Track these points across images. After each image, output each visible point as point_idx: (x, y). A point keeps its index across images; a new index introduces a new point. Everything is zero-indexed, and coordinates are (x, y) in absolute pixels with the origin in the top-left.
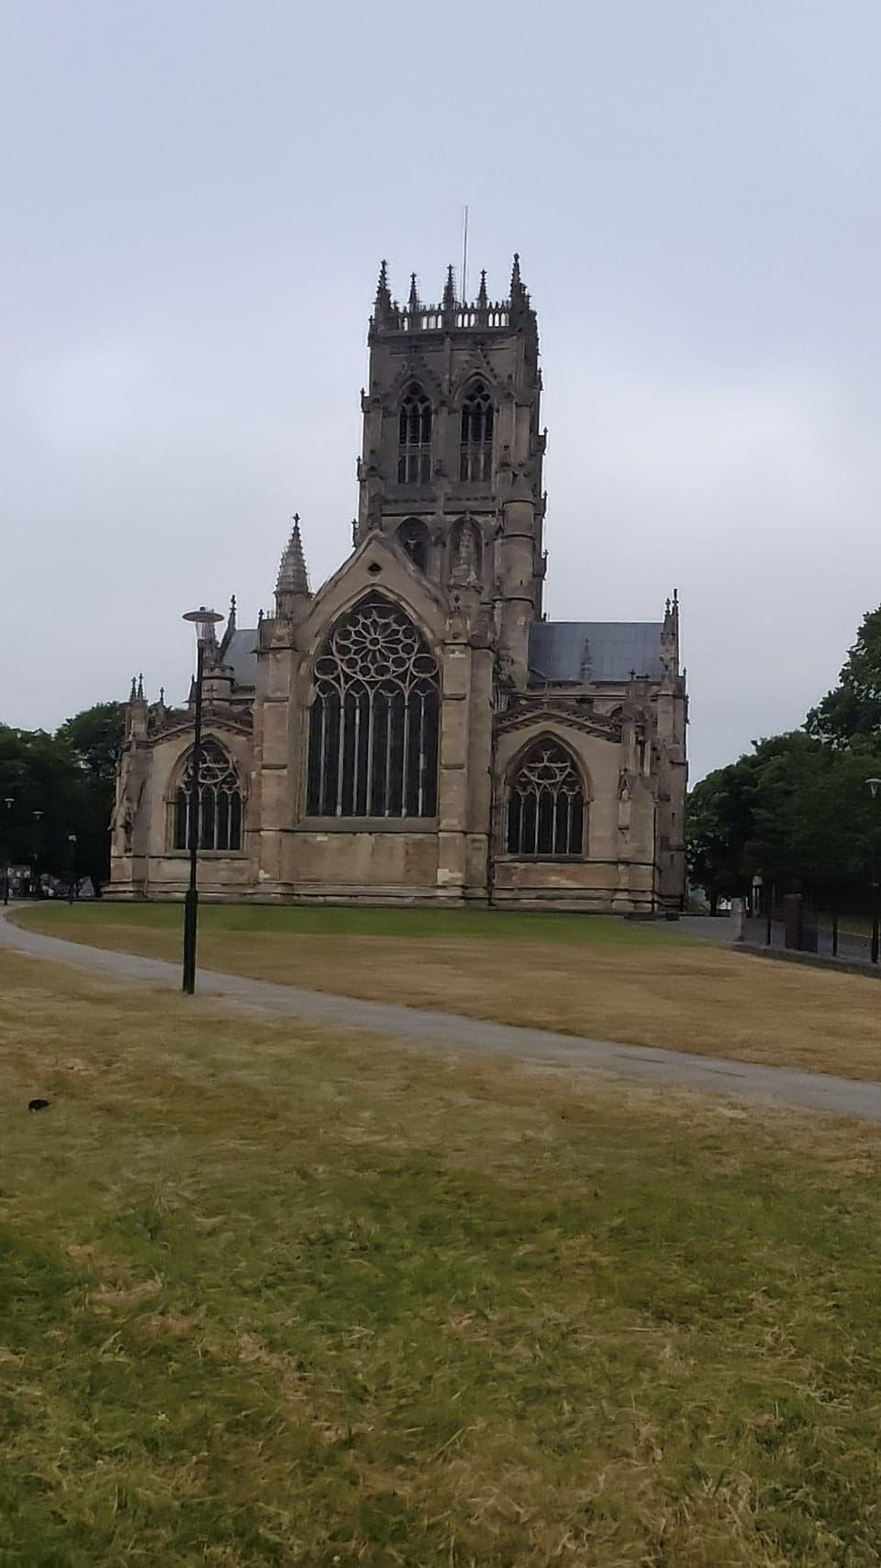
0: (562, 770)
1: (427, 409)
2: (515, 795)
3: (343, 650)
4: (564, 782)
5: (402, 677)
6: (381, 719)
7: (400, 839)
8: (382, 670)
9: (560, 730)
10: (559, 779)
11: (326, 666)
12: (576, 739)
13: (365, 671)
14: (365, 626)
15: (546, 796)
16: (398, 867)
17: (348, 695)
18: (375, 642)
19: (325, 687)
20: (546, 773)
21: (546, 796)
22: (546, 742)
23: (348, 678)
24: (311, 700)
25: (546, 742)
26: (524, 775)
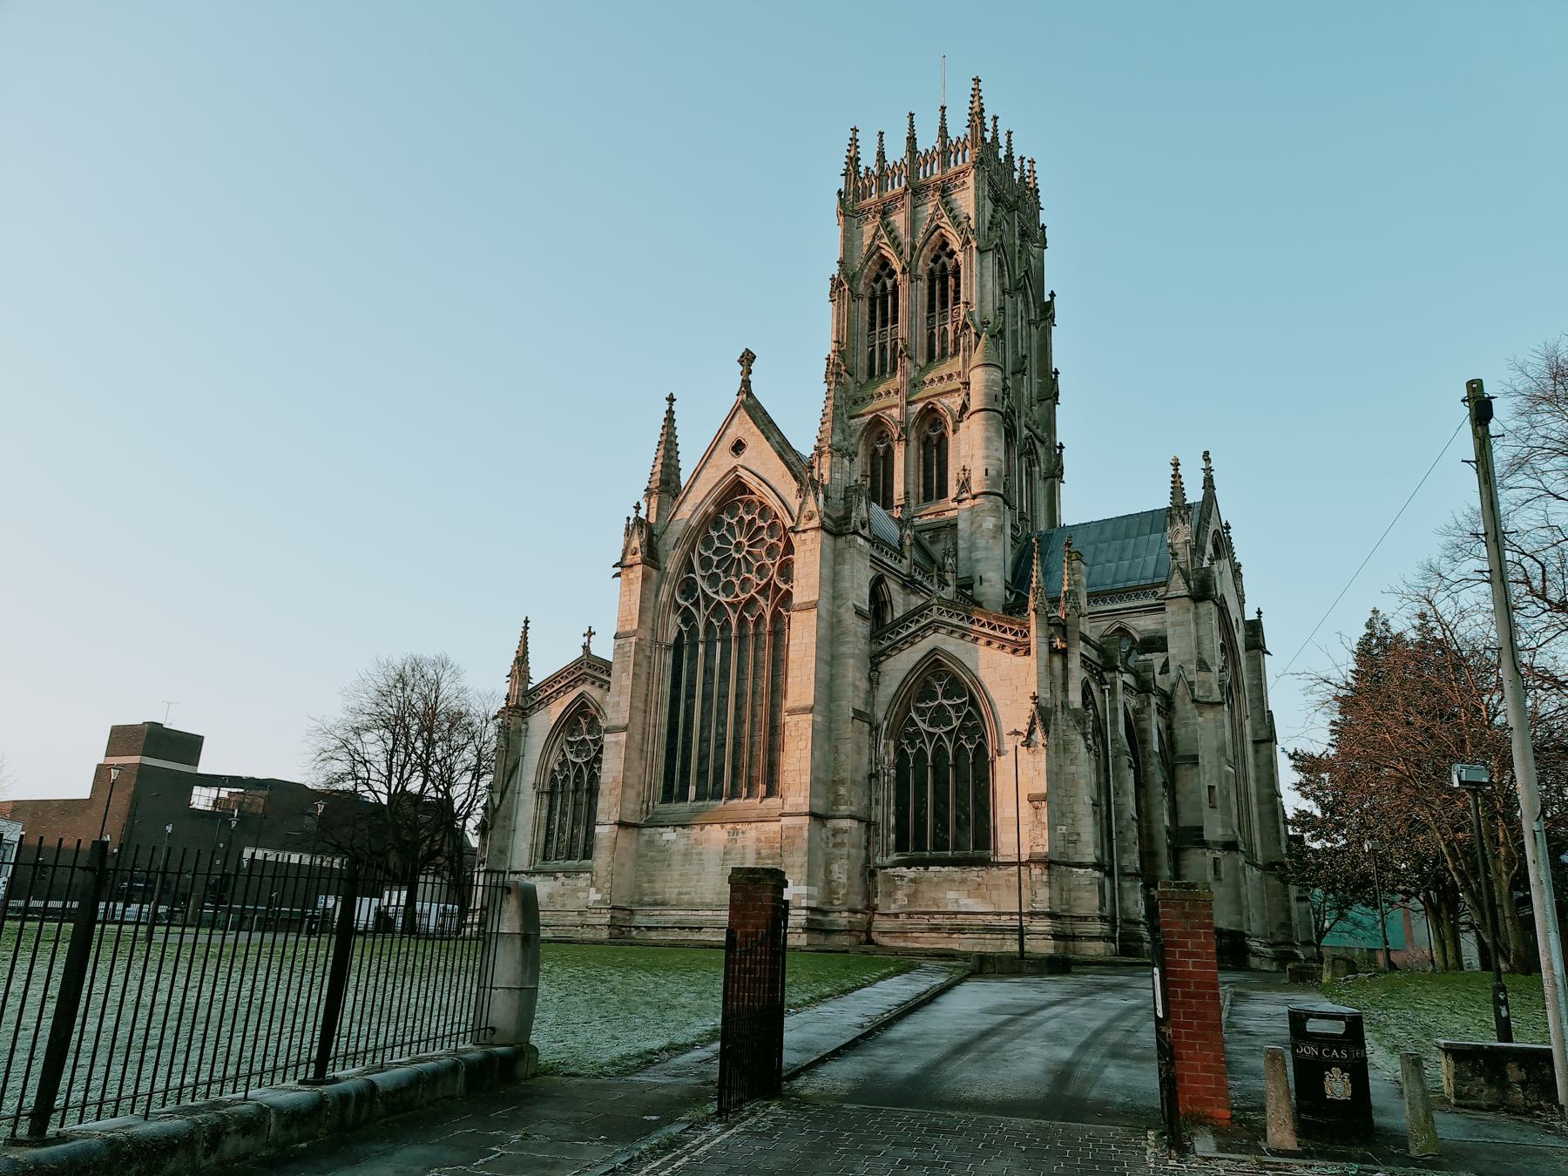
0: (958, 708)
2: (901, 753)
3: (706, 563)
4: (962, 728)
5: (763, 591)
9: (951, 645)
10: (956, 723)
11: (688, 588)
14: (730, 527)
15: (939, 751)
17: (709, 625)
18: (739, 546)
19: (688, 618)
21: (939, 751)
22: (934, 664)
25: (934, 664)
26: (912, 723)
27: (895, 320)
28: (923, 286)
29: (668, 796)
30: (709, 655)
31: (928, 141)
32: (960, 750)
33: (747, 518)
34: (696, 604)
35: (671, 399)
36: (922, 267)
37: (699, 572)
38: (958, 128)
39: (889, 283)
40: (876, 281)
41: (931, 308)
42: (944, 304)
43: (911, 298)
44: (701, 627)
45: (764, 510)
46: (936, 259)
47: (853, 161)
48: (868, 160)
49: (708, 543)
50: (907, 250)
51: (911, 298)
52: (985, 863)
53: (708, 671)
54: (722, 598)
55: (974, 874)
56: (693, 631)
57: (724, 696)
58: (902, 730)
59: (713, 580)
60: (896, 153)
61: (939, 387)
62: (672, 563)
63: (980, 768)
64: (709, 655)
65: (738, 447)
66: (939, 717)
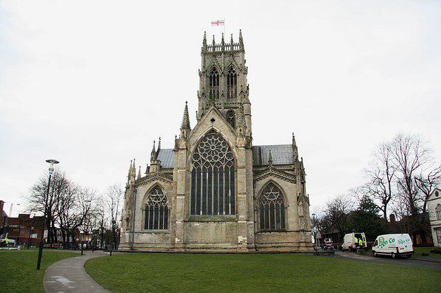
0: (276, 194)
1: (218, 76)
3: (202, 151)
5: (222, 160)
6: (216, 176)
7: (224, 224)
8: (216, 158)
9: (275, 179)
12: (282, 183)
13: (210, 158)
14: (209, 142)
15: (272, 204)
16: (222, 235)
17: (204, 168)
18: (213, 147)
19: (196, 164)
20: (272, 196)
21: (272, 204)
22: (271, 184)
23: (204, 161)
24: (191, 169)
25: (271, 184)
27: (218, 85)
28: (226, 77)
29: (193, 212)
30: (204, 176)
31: (227, 41)
32: (277, 205)
33: (215, 140)
34: (200, 161)
35: (187, 102)
36: (226, 72)
37: (200, 153)
38: (236, 41)
39: (216, 75)
40: (212, 73)
41: (228, 84)
42: (232, 84)
43: (223, 81)
44: (202, 167)
45: (221, 139)
46: (230, 72)
47: (205, 40)
48: (209, 43)
49: (202, 145)
50: (223, 68)
51: (223, 81)
52: (286, 231)
53: (204, 180)
54: (208, 161)
55: (283, 234)
56: (199, 169)
57: (210, 188)
58: (262, 199)
59: (205, 155)
60: (218, 42)
61: (233, 105)
62: (192, 150)
63: (283, 208)
64: (204, 176)
65: (213, 120)
66: (272, 196)
